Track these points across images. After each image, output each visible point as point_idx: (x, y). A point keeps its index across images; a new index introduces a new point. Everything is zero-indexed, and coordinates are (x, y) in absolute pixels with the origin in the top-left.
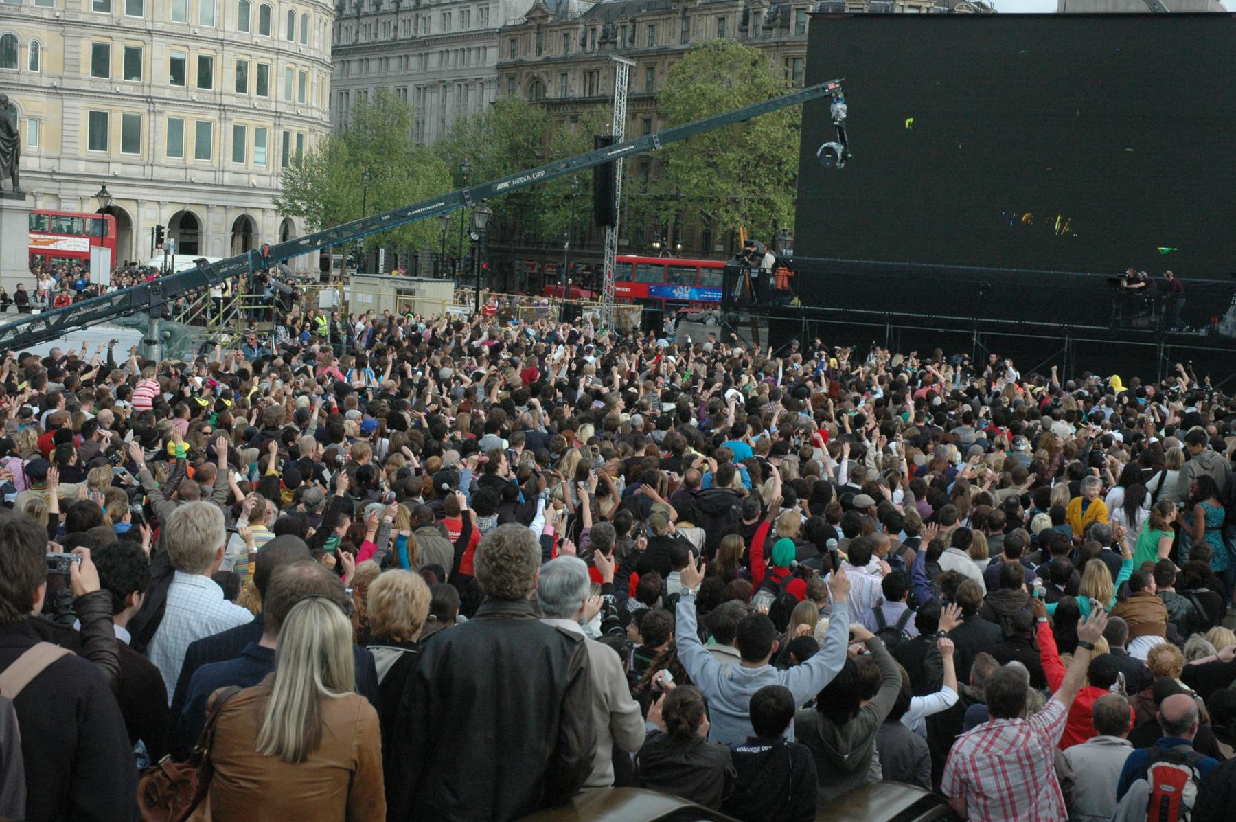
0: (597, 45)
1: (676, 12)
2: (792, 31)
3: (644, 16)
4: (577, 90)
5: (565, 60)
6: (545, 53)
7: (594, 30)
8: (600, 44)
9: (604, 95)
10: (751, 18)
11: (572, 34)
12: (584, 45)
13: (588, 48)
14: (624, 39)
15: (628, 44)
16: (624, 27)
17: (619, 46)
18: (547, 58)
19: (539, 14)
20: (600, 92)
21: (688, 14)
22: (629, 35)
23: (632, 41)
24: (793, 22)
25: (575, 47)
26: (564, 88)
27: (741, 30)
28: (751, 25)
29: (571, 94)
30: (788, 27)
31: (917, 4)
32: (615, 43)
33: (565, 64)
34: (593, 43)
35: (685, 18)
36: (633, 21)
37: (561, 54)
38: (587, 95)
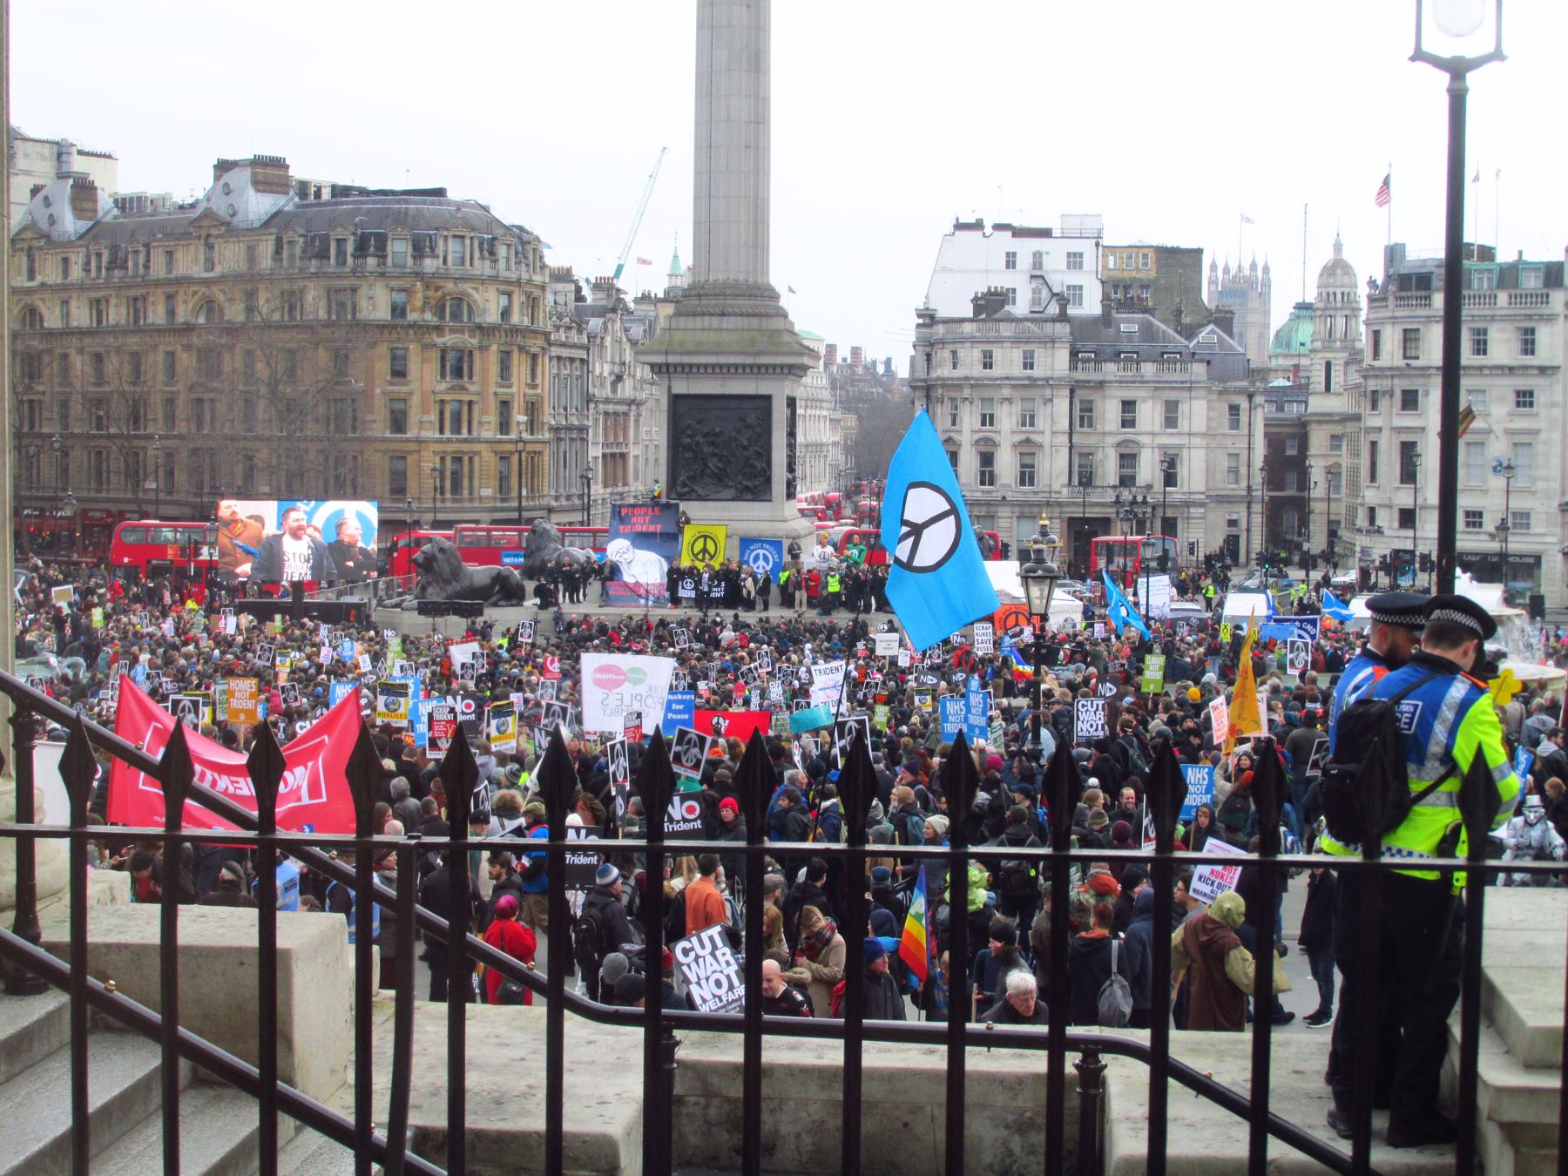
0: (103, 270)
1: (199, 238)
2: (333, 261)
3: (160, 240)
4: (81, 316)
5: (63, 288)
6: (39, 279)
7: (99, 255)
8: (108, 269)
9: (117, 325)
10: (285, 247)
11: (73, 258)
12: (88, 271)
13: (93, 274)
14: (136, 265)
15: (141, 271)
16: (136, 252)
17: (130, 272)
18: (43, 284)
19: (29, 235)
20: (112, 322)
21: (211, 240)
22: (142, 260)
23: (147, 267)
24: (333, 252)
25: (76, 273)
26: (66, 315)
27: (274, 260)
28: (285, 254)
29: (75, 324)
30: (329, 258)
32: (126, 268)
33: (63, 291)
34: (99, 268)
35: (210, 247)
36: (147, 246)
37: (59, 280)
38: (94, 325)
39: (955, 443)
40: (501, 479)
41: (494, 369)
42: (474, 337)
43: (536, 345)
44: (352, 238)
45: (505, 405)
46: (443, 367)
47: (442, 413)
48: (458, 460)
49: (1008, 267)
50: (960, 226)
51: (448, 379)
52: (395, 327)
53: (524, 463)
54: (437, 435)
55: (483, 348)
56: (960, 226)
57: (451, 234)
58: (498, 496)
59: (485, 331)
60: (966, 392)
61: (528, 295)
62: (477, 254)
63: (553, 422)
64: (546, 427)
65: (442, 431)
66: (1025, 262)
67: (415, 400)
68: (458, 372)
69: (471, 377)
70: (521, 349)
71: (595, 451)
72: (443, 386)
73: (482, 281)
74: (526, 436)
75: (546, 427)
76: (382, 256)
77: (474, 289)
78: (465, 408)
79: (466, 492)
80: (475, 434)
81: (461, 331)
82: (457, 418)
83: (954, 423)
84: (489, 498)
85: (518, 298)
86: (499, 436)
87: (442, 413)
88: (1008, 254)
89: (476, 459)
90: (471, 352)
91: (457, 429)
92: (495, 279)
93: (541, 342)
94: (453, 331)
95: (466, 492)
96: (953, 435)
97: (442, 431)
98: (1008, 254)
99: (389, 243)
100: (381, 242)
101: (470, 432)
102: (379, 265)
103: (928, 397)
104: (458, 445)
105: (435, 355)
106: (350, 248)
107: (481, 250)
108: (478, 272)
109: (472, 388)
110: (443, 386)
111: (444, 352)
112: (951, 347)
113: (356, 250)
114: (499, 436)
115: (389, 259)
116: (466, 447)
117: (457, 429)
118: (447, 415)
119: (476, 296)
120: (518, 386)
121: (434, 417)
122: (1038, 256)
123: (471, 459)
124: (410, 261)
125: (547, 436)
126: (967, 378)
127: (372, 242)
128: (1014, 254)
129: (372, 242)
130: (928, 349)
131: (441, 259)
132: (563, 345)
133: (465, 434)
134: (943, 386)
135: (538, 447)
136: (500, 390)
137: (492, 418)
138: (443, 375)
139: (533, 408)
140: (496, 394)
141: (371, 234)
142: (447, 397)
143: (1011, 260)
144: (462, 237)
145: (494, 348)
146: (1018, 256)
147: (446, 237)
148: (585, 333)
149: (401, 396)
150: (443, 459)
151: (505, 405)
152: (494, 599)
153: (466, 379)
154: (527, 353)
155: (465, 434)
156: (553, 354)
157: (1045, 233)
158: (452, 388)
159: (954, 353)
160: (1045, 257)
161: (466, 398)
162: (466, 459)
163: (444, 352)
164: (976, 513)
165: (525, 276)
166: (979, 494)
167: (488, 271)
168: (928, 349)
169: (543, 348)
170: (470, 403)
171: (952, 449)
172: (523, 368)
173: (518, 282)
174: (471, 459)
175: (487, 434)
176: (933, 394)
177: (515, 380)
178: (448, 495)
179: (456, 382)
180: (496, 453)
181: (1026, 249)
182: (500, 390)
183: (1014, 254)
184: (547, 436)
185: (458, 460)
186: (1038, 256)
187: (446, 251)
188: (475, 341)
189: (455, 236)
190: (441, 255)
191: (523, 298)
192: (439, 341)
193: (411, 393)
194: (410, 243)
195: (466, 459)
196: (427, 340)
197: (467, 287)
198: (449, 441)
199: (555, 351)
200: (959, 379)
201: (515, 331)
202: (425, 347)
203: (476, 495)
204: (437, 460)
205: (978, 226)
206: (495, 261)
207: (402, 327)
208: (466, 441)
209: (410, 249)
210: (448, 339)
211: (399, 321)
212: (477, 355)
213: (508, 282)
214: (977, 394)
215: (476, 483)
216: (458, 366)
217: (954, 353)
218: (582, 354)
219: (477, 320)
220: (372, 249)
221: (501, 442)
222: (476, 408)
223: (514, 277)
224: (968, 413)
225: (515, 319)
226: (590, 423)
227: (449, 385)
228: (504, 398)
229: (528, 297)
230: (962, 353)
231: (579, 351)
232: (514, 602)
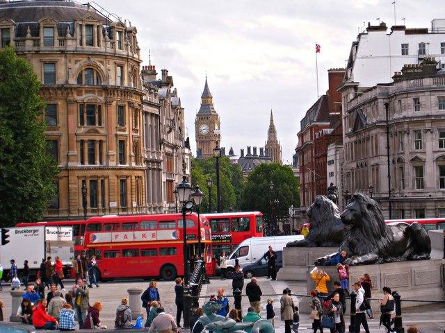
31: (92, 23)
39: (421, 160)
40: (122, 195)
41: (114, 118)
42: (102, 96)
43: (136, 100)
44: (14, 27)
45: (122, 144)
46: (82, 117)
47: (82, 150)
48: (94, 182)
49: (403, 54)
50: (370, 28)
51: (86, 125)
52: (48, 89)
53: (134, 184)
54: (79, 165)
55: (107, 104)
56: (370, 28)
57: (84, 23)
58: (120, 207)
59: (107, 90)
60: (428, 126)
61: (133, 67)
62: (102, 38)
63: (146, 157)
64: (143, 159)
65: (82, 163)
66: (413, 50)
67: (63, 141)
68: (92, 122)
69: (100, 124)
70: (130, 104)
71: (164, 178)
72: (82, 130)
73: (105, 56)
74: (134, 164)
75: (143, 159)
76: (37, 43)
77: (100, 62)
78: (97, 145)
79: (100, 204)
80: (105, 164)
81: (93, 92)
82: (92, 151)
83: (417, 148)
84: (114, 208)
85: (127, 69)
86: (119, 165)
87: (82, 150)
88: (403, 45)
89: (106, 181)
90: (100, 106)
91: (92, 161)
92: (114, 56)
93: (138, 101)
94: (87, 92)
95: (100, 204)
96: (418, 155)
97: (82, 163)
98: (403, 45)
99: (41, 30)
100: (36, 32)
101: (101, 163)
102: (34, 45)
103: (388, 133)
104: (94, 172)
105: (75, 109)
106: (12, 35)
107: (104, 35)
108: (104, 50)
109: (102, 131)
110: (82, 130)
111: (82, 106)
112: (414, 96)
113: (18, 35)
114: (119, 165)
115: (42, 41)
116: (99, 173)
117: (92, 161)
118: (86, 151)
119: (102, 67)
120: (128, 132)
121: (76, 152)
122: (422, 46)
123: (102, 181)
124: (57, 42)
125: (144, 166)
126: (428, 116)
127: (29, 30)
128: (407, 45)
129: (29, 30)
130: (387, 101)
131: (78, 41)
132: (150, 104)
133: (98, 164)
134: (408, 123)
135: (140, 173)
136: (118, 133)
137: (114, 152)
138: (82, 123)
139: (136, 147)
140: (116, 135)
141: (27, 25)
142: (86, 138)
143: (405, 49)
144: (92, 26)
145: (114, 103)
146: (409, 47)
147: (81, 25)
148: (157, 97)
149: (53, 138)
150: (84, 181)
151: (122, 144)
152: (407, 253)
153: (97, 125)
154: (133, 107)
155: (98, 164)
156: (144, 109)
157: (424, 31)
158: (89, 132)
159: (417, 100)
160: (426, 46)
161: (98, 138)
162: (100, 181)
163: (82, 106)
164: (439, 207)
165: (130, 54)
166: (441, 194)
167: (109, 50)
168: (387, 101)
169: (140, 105)
170: (100, 141)
171: (418, 164)
172: (131, 118)
173: (127, 58)
174: (102, 181)
175: (112, 164)
176: (391, 130)
177: (127, 126)
178: (89, 207)
179: (91, 127)
180: (118, 176)
181: (414, 41)
182: (118, 133)
183: (407, 45)
184: (144, 166)
185: (94, 182)
186: (422, 47)
187: (81, 36)
188: (102, 98)
189: (87, 25)
190: (79, 37)
191: (129, 69)
192: (79, 98)
193: (60, 136)
194: (56, 30)
195: (100, 181)
196: (70, 97)
197: (95, 60)
198: (89, 169)
199: (146, 108)
200: (423, 117)
201: (127, 92)
202: (69, 103)
203: (107, 207)
204: (81, 181)
205: (382, 27)
206: (113, 44)
207: (53, 89)
208: (99, 169)
209: (56, 34)
210: (86, 97)
211: (51, 84)
212: (103, 108)
213: (121, 58)
214: (435, 127)
215: (106, 198)
216: (91, 114)
217: (417, 100)
218: (156, 111)
219: (103, 84)
220: (29, 35)
221: (121, 169)
222: (104, 145)
223: (124, 52)
224: (430, 139)
225: (126, 84)
226: (161, 158)
227: (87, 129)
228: (121, 138)
229: (132, 70)
230: (422, 99)
231: (155, 109)
232: (425, 256)
